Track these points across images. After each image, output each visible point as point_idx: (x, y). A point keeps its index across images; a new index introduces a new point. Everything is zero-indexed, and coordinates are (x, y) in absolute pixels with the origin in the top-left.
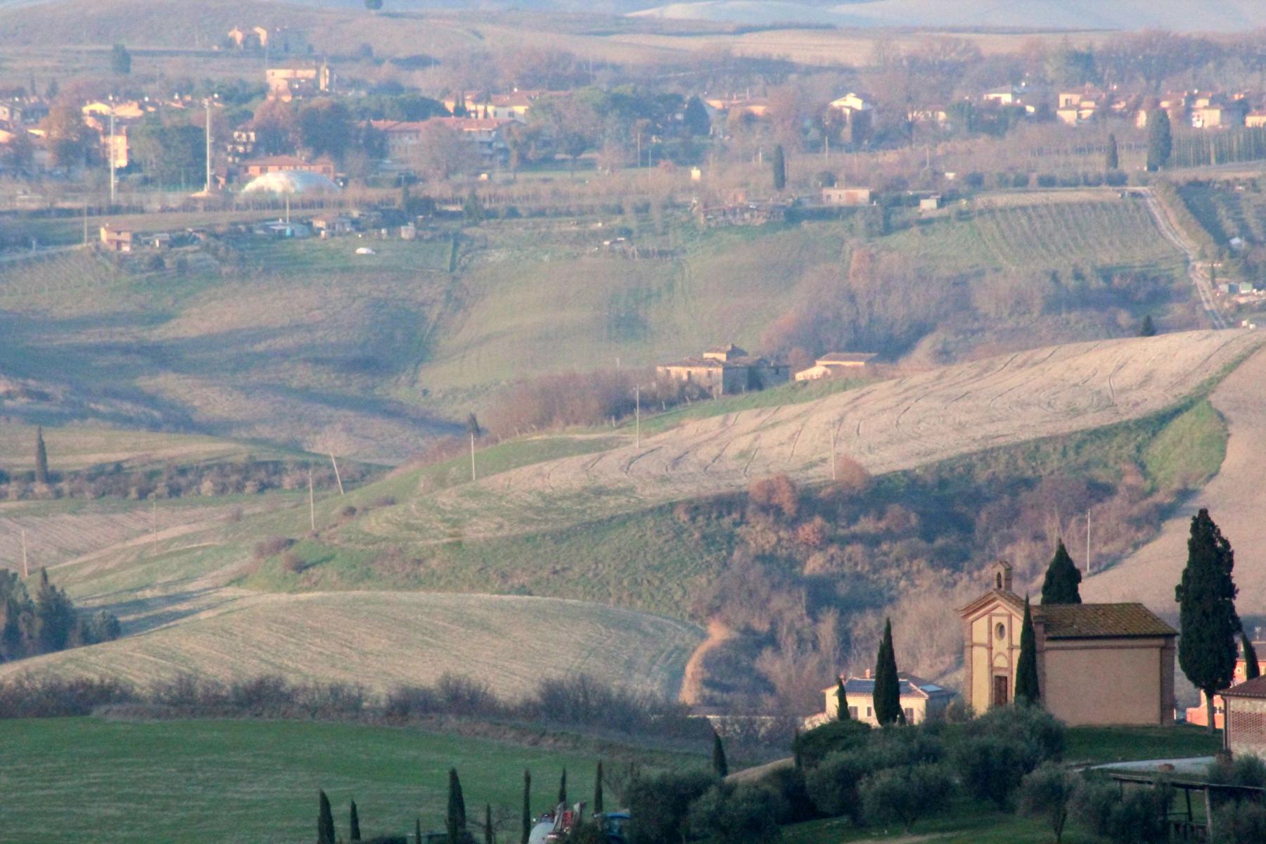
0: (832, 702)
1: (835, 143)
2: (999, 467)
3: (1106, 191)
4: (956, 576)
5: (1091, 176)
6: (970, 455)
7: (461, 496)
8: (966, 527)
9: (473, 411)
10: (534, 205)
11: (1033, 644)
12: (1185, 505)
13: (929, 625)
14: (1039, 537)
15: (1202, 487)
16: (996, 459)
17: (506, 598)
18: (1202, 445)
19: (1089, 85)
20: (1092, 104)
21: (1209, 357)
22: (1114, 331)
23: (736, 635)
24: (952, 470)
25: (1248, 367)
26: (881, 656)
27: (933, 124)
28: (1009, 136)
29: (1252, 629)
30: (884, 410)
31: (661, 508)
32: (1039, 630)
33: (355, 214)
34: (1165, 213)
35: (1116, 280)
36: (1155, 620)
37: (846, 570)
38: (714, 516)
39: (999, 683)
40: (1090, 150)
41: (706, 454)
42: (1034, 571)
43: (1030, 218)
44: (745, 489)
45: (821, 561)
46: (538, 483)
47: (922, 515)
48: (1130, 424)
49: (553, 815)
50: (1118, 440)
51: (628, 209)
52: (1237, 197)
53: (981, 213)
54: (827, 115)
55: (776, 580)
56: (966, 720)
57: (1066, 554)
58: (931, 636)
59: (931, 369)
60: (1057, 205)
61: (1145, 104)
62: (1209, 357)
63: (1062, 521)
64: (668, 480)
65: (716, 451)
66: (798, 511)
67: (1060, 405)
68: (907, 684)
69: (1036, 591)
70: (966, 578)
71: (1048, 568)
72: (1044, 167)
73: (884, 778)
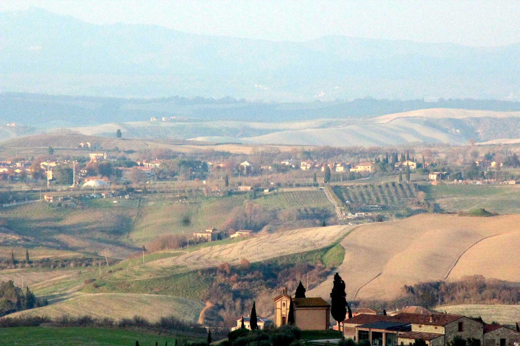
0: (239, 324)
1: (242, 174)
2: (284, 261)
4: (272, 290)
5: (309, 184)
6: (277, 258)
7: (140, 268)
8: (275, 277)
9: (144, 245)
10: (161, 190)
11: (293, 308)
12: (333, 272)
13: (265, 303)
14: (294, 280)
16: (284, 259)
17: (153, 295)
18: (338, 256)
19: (309, 160)
20: (310, 165)
22: (315, 225)
23: (213, 305)
24: (272, 262)
25: (349, 235)
26: (252, 312)
27: (268, 170)
28: (288, 173)
29: (350, 305)
30: (254, 245)
31: (194, 271)
32: (294, 304)
33: (113, 192)
35: (316, 212)
36: (325, 302)
37: (243, 288)
38: (208, 273)
39: (283, 319)
40: (309, 177)
41: (206, 257)
42: (293, 289)
43: (293, 195)
44: (216, 266)
45: (237, 286)
46: (161, 264)
47: (264, 274)
48: (319, 250)
50: (315, 254)
51: (186, 191)
52: (348, 190)
53: (280, 193)
54: (240, 167)
55: (225, 290)
58: (265, 306)
59: (265, 235)
60: (300, 192)
61: (324, 165)
63: (301, 276)
64: (196, 264)
65: (209, 256)
66: (230, 272)
67: (301, 245)
68: (259, 319)
69: (294, 294)
70: (275, 291)
71: (297, 288)
72: (297, 181)
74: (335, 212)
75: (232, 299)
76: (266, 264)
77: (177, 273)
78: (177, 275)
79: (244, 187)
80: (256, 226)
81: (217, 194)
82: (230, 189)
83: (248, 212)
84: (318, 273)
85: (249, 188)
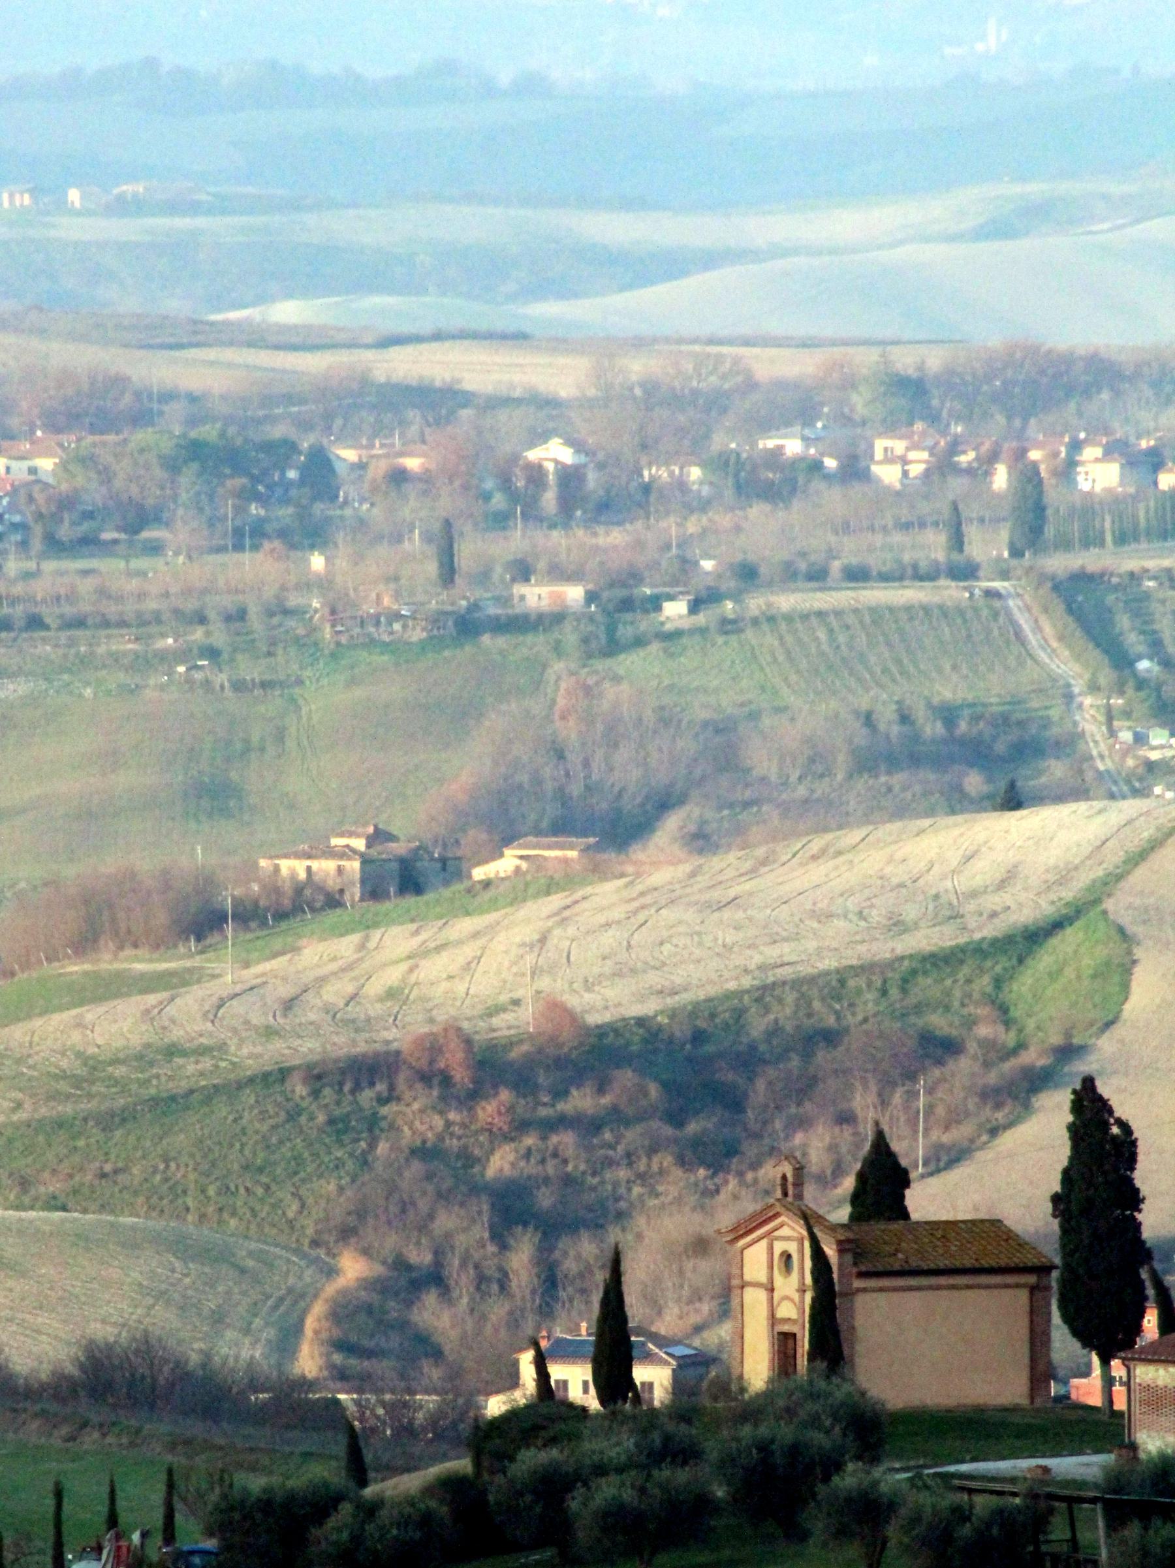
1: (533, 513)
2: (784, 1013)
3: (947, 588)
5: (923, 565)
6: (739, 994)
8: (734, 1102)
10: (68, 610)
12: (1066, 1069)
14: (846, 1118)
15: (1093, 1040)
16: (780, 1001)
18: (1094, 976)
19: (919, 426)
20: (925, 455)
21: (1104, 843)
23: (379, 1270)
25: (1157, 859)
26: (605, 1303)
27: (682, 485)
28: (796, 504)
30: (608, 925)
31: (266, 1076)
34: (1036, 621)
35: (963, 726)
38: (347, 1087)
39: (784, 1342)
40: (922, 525)
41: (334, 993)
42: (838, 1170)
43: (831, 631)
44: (395, 1046)
45: (511, 1157)
46: (76, 1037)
47: (665, 1085)
48: (985, 946)
49: (99, 1549)
50: (965, 971)
51: (212, 615)
52: (1147, 596)
53: (755, 622)
54: (518, 471)
56: (736, 1399)
57: (887, 1146)
58: (681, 1272)
61: (1003, 456)
62: (1104, 843)
63: (880, 1095)
64: (277, 1033)
65: (350, 989)
66: (475, 1081)
67: (876, 916)
68: (643, 1344)
70: (733, 1183)
71: (858, 1166)
72: (851, 551)
73: (607, 1490)
74: (1075, 724)
75: (486, 1235)
76: (681, 1032)
77: (171, 1085)
78: (173, 1098)
79: (545, 590)
80: (619, 811)
81: (391, 633)
82: (464, 603)
83: (569, 731)
84: (980, 1082)
85: (574, 594)
